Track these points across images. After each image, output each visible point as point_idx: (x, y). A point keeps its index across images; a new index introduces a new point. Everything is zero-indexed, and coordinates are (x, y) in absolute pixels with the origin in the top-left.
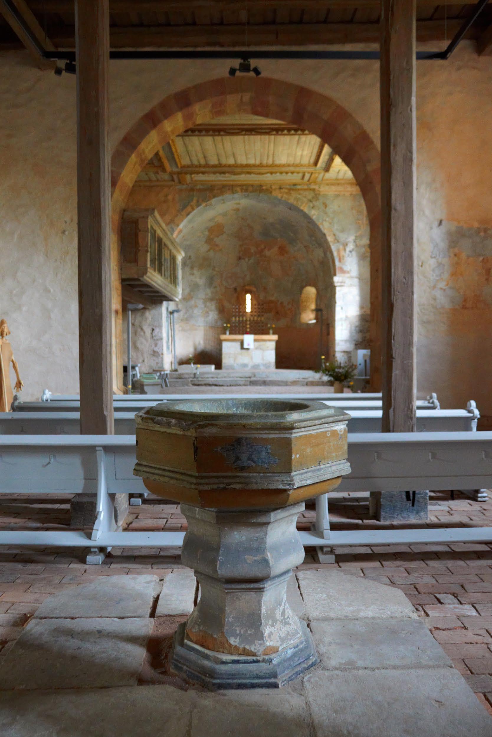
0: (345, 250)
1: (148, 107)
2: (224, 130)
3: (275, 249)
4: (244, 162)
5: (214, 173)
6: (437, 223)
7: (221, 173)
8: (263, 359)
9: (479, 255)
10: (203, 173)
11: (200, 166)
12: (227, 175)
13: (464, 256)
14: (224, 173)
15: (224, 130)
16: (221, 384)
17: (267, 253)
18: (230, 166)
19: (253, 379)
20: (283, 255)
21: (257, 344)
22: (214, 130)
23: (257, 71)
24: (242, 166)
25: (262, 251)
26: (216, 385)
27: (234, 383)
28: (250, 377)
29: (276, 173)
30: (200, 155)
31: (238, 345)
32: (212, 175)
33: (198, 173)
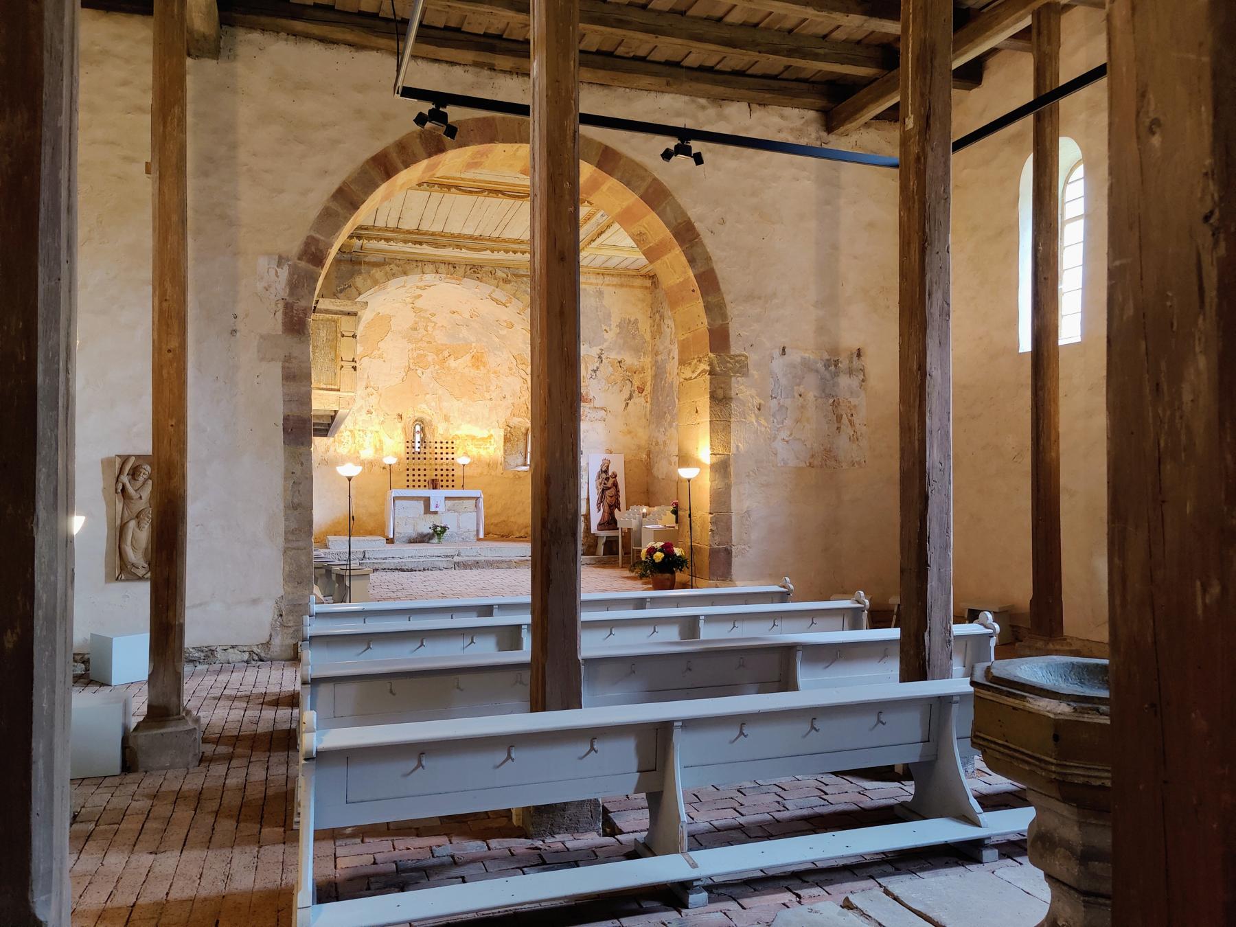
0: (587, 368)
1: (377, 147)
2: (456, 187)
3: (469, 356)
4: (456, 231)
5: (405, 242)
6: (777, 352)
7: (415, 243)
8: (459, 527)
9: (829, 396)
10: (387, 240)
11: (386, 229)
12: (424, 246)
13: (811, 396)
14: (421, 243)
15: (456, 187)
16: (410, 566)
17: (452, 363)
18: (433, 234)
19: (456, 559)
20: (478, 367)
21: (450, 503)
22: (441, 185)
23: (698, 159)
24: (453, 236)
25: (444, 360)
26: (402, 570)
27: (430, 566)
28: (452, 556)
29: (499, 251)
30: (394, 215)
31: (421, 504)
32: (401, 244)
33: (379, 239)
